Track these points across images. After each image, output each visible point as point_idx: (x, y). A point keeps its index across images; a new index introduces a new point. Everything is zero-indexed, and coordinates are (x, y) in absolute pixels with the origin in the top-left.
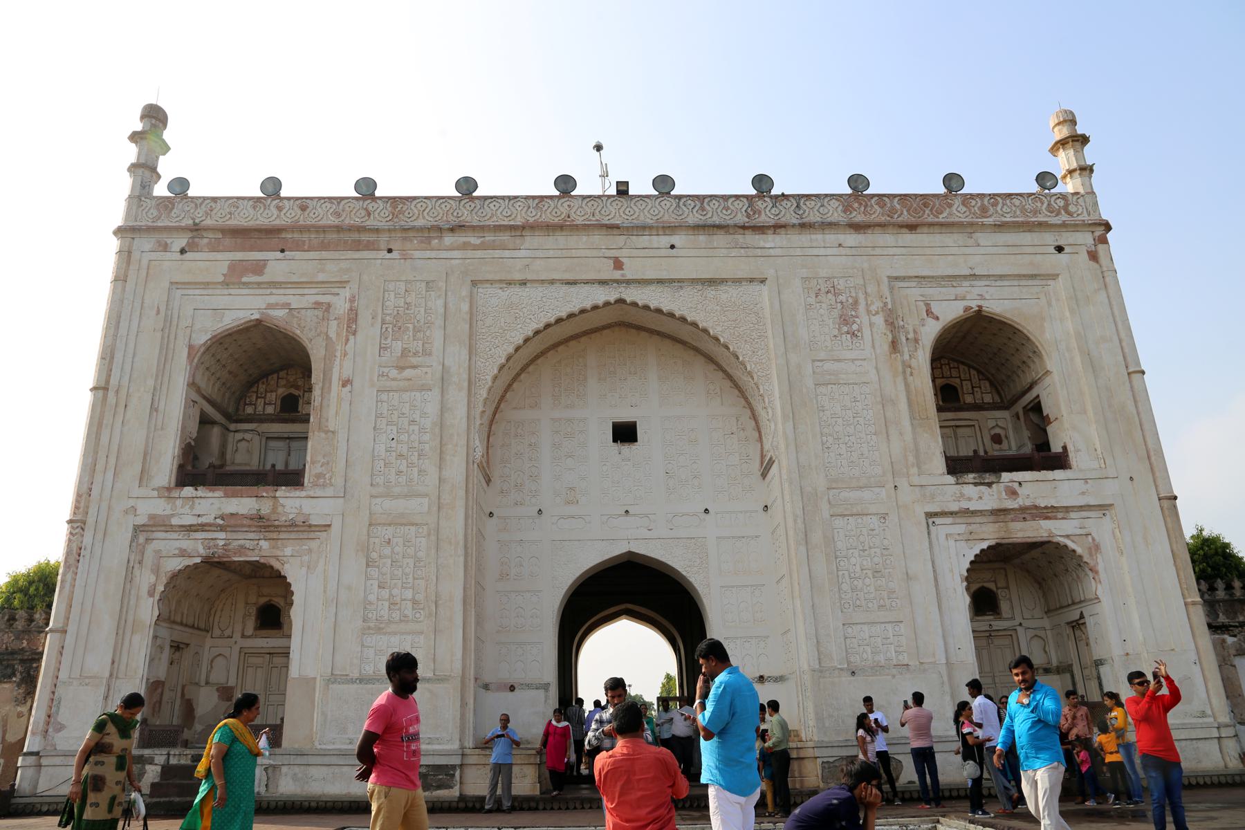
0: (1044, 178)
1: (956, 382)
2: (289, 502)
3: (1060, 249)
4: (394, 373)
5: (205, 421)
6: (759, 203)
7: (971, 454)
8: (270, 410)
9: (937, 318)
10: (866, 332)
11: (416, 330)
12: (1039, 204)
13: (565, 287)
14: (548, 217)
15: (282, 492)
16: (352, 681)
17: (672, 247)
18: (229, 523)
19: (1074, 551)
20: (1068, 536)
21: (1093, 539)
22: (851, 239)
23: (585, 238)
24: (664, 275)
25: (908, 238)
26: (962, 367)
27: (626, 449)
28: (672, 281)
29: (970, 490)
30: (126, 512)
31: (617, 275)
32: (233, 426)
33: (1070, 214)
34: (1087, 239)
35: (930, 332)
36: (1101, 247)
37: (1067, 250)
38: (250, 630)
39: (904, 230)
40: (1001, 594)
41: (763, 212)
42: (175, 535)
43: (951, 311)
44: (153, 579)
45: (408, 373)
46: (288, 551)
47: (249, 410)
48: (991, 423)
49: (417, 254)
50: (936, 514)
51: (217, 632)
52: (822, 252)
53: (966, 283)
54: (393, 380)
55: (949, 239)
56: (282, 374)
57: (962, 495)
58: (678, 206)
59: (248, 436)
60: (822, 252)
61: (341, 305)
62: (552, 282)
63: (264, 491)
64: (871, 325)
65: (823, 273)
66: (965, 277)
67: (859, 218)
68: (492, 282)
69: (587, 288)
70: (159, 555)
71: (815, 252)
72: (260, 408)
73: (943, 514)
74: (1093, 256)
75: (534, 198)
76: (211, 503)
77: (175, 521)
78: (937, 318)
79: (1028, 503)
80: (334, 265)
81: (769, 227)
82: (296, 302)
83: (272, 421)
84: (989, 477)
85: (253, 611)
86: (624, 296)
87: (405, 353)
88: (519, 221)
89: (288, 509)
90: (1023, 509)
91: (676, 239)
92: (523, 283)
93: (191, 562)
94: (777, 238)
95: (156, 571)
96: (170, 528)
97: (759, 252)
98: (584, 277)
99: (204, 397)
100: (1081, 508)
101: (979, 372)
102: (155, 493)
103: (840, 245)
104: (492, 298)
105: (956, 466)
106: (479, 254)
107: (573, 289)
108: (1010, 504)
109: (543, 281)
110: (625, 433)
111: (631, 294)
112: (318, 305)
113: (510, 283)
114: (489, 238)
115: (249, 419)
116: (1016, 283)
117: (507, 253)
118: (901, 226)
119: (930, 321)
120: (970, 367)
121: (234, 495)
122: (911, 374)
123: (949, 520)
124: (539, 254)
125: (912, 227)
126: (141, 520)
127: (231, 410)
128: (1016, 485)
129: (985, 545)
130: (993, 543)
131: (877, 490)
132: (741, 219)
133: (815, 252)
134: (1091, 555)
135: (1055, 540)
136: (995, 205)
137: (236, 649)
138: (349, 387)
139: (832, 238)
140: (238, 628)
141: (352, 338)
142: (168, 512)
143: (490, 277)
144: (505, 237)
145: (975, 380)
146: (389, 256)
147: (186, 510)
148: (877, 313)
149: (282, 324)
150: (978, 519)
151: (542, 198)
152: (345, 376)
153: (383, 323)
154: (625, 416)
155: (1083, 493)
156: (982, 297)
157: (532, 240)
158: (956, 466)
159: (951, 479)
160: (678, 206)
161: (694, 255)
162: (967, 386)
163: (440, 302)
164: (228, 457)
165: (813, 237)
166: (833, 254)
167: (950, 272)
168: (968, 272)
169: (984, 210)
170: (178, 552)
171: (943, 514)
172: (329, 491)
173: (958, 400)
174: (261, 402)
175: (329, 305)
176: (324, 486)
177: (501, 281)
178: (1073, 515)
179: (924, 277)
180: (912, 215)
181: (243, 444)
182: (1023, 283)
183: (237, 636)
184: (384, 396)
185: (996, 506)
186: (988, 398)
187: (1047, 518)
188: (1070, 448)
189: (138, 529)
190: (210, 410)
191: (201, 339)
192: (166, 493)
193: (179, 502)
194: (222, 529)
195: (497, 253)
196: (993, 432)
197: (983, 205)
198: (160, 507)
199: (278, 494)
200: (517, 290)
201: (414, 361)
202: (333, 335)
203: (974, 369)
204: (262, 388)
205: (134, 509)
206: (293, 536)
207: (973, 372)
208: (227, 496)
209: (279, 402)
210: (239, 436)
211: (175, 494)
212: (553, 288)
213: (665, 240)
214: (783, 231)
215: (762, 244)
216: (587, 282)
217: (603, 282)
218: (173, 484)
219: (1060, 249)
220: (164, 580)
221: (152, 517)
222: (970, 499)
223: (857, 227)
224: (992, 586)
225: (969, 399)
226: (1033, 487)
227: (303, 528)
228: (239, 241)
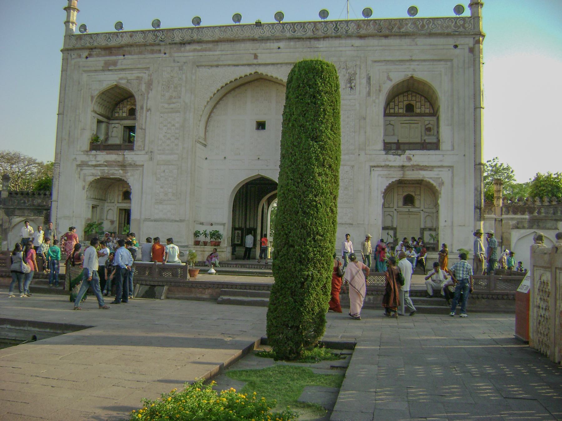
0: (459, 9)
1: (413, 103)
2: (129, 156)
3: (456, 47)
4: (166, 106)
5: (99, 122)
6: (319, 25)
7: (396, 141)
8: (124, 115)
9: (391, 80)
10: (357, 86)
11: (176, 87)
12: (450, 23)
13: (234, 67)
14: (228, 35)
15: (126, 152)
16: (152, 221)
17: (279, 48)
18: (109, 164)
19: (432, 185)
20: (431, 178)
21: (442, 180)
22: (358, 42)
23: (243, 45)
24: (275, 61)
25: (384, 41)
26: (418, 96)
27: (262, 132)
28: (277, 64)
29: (391, 157)
30: (73, 160)
31: (255, 62)
32: (111, 122)
33: (464, 27)
34: (470, 42)
35: (387, 87)
36: (477, 45)
37: (459, 47)
38: (120, 201)
39: (382, 38)
40: (416, 197)
42: (90, 168)
43: (398, 75)
44: (84, 184)
45: (172, 106)
46: (129, 174)
47: (117, 115)
48: (427, 122)
49: (176, 55)
50: (375, 167)
51: (109, 201)
52: (344, 49)
53: (408, 63)
54: (166, 109)
55: (406, 41)
56: (129, 100)
57: (387, 159)
58: (283, 28)
59: (117, 125)
60: (344, 49)
61: (145, 76)
62: (229, 65)
63: (120, 152)
64: (360, 84)
65: (343, 59)
66: (408, 61)
67: (363, 32)
68: (205, 66)
69: (243, 68)
70: (85, 175)
71: (341, 49)
72: (121, 114)
73: (378, 166)
74: (472, 50)
75: (223, 26)
76: (103, 157)
77: (90, 163)
78: (391, 80)
79: (415, 164)
81: (321, 38)
82: (129, 77)
83: (125, 119)
84: (400, 152)
85: (121, 193)
86: (257, 71)
87: (171, 98)
88: (216, 38)
89: (129, 159)
90: (413, 166)
91: (282, 44)
92: (217, 66)
93: (96, 178)
94: (325, 42)
95: (84, 181)
96: (89, 166)
97: (316, 49)
98: (242, 63)
99: (98, 114)
100: (439, 167)
101: (425, 98)
102: (82, 153)
103: (352, 46)
104: (204, 72)
105: (388, 147)
106: (200, 53)
107: (237, 68)
108: (406, 164)
109: (225, 65)
110: (261, 125)
112: (138, 77)
113: (212, 66)
114: (204, 46)
115: (116, 119)
116: (431, 63)
117: (211, 53)
118: (381, 36)
119: (388, 82)
120: (421, 95)
121: (110, 154)
122: (375, 106)
123: (381, 169)
124: (224, 53)
125: (386, 36)
126: (79, 163)
127: (110, 116)
128: (411, 156)
129: (394, 180)
130: (398, 179)
131: (351, 155)
132: (310, 34)
133: (341, 49)
134: (439, 186)
135: (425, 179)
136: (428, 24)
137: (116, 207)
138: (149, 112)
139: (349, 42)
140: (116, 199)
141: (150, 91)
142: (88, 160)
143: (204, 64)
144: (210, 46)
145: (423, 102)
146: (165, 56)
147: (94, 159)
148: (364, 78)
149: (124, 86)
150: (392, 169)
151: (227, 26)
152: (148, 108)
153: (163, 85)
154: (261, 119)
155: (441, 161)
156: (414, 70)
157: (222, 46)
158: (388, 147)
159: (383, 152)
160: (283, 28)
162: (418, 105)
163: (184, 76)
164: (110, 134)
165: (341, 41)
167: (400, 58)
168: (408, 58)
169: (423, 26)
170: (92, 174)
171: (378, 166)
172: (143, 152)
173: (413, 111)
174: (121, 111)
175: (142, 77)
176: (141, 150)
177: (208, 66)
178: (435, 169)
179: (388, 61)
180: (389, 30)
181: (115, 129)
182: (435, 63)
183: (116, 202)
184: (162, 115)
185: (401, 164)
186: (427, 111)
187: (425, 170)
188: (441, 141)
189: (78, 166)
190: (101, 118)
191: (96, 93)
192: (86, 152)
193: (91, 156)
194: (106, 166)
195: (207, 53)
196: (427, 127)
197: (423, 24)
198: (85, 158)
199: (125, 153)
200: (214, 69)
201: (174, 100)
202: (143, 90)
203: (424, 96)
204: (121, 106)
205: (76, 158)
206: (131, 168)
207: (423, 98)
208: (107, 154)
209: (128, 111)
210: (113, 125)
211: (89, 153)
212: (229, 68)
213: (276, 45)
214: (327, 39)
215: (317, 46)
216: (243, 65)
217: (249, 65)
218: (89, 149)
219: (456, 47)
220: (88, 184)
221: (82, 162)
222: (390, 161)
223: (361, 37)
224: (413, 194)
225: (418, 111)
226: (420, 157)
227: (134, 166)
228: (107, 52)
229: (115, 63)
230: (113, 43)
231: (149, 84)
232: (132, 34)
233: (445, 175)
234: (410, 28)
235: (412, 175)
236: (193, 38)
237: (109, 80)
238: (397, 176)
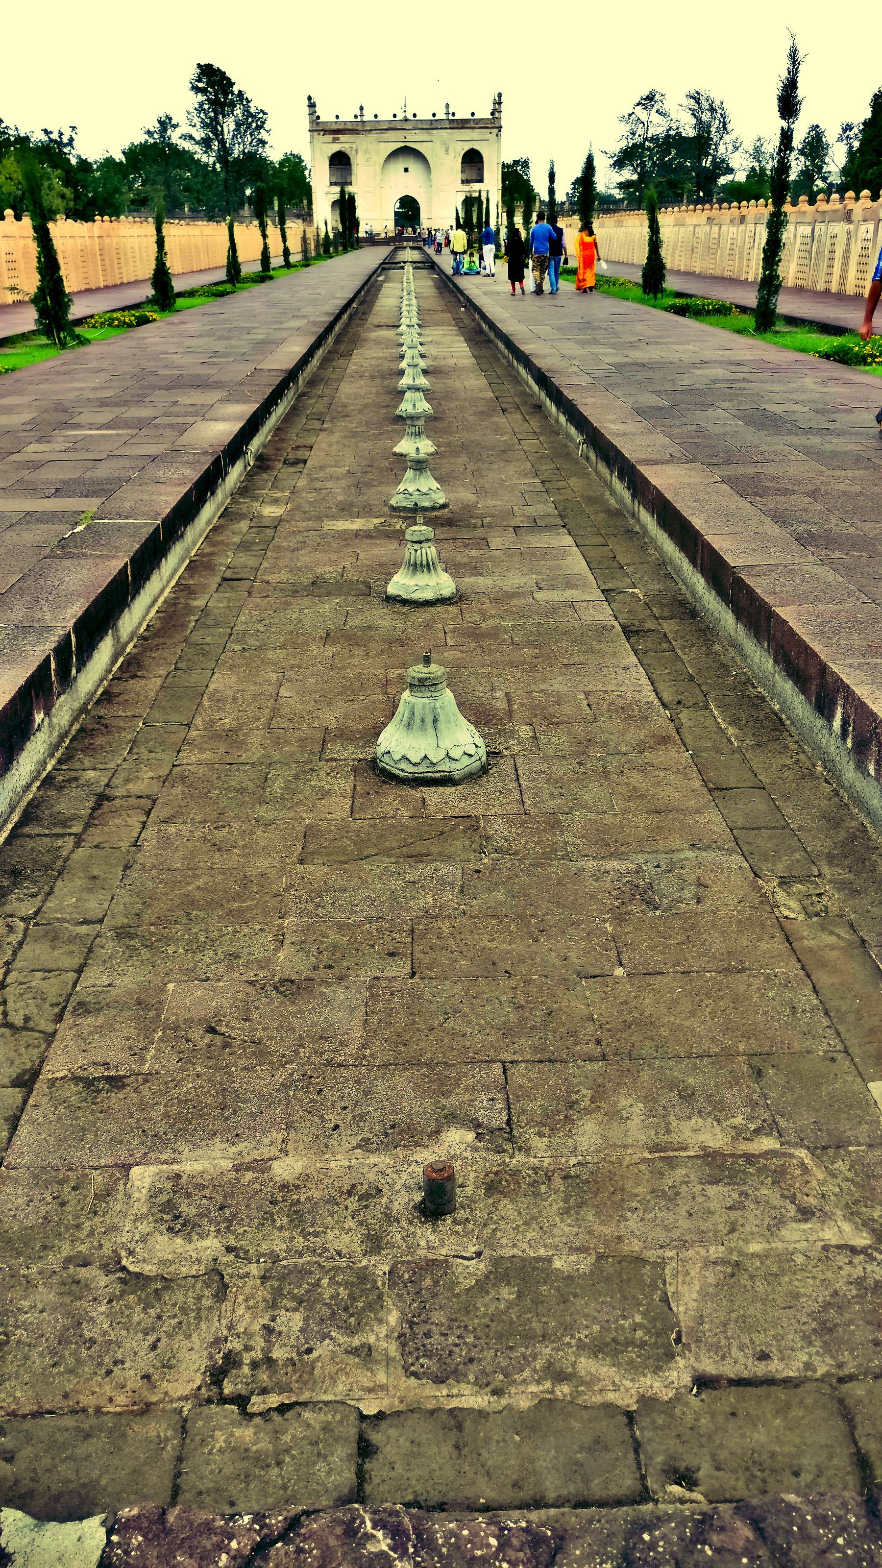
14: (392, 126)
41: (433, 125)
43: (467, 148)
105: (463, 182)
110: (406, 170)
111: (409, 144)
161: (419, 135)
180: (463, 124)
226: (476, 186)
229: (338, 139)
230: (335, 127)
231: (357, 151)
232: (345, 123)
234: (472, 125)
237: (336, 148)
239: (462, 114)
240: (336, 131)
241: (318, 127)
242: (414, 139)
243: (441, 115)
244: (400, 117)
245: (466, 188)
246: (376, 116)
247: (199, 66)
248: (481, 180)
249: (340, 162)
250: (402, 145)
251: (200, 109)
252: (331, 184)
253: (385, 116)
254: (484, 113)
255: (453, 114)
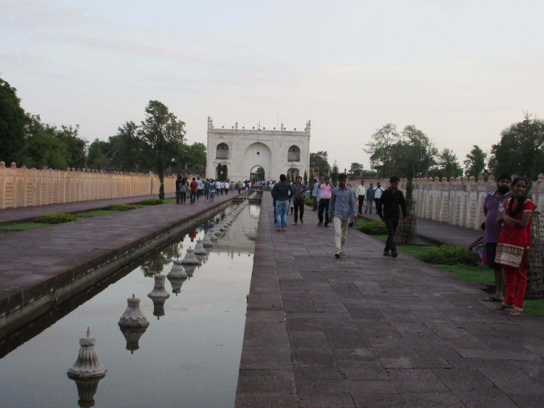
2: (227, 161)
41: (273, 133)
43: (291, 145)
76: (220, 161)
80: (230, 137)
105: (288, 161)
110: (258, 153)
161: (266, 138)
166: (280, 138)
180: (290, 134)
226: (296, 163)
227: (229, 163)
231: (232, 143)
232: (227, 130)
233: (301, 167)
235: (294, 167)
236: (244, 133)
237: (221, 141)
238: (290, 167)
239: (289, 129)
240: (221, 133)
241: (212, 132)
242: (263, 139)
243: (279, 129)
244: (256, 128)
245: (290, 164)
246: (243, 128)
247: (151, 101)
248: (298, 160)
249: (223, 147)
250: (257, 141)
251: (149, 121)
252: (217, 158)
253: (249, 127)
254: (301, 128)
255: (285, 129)
